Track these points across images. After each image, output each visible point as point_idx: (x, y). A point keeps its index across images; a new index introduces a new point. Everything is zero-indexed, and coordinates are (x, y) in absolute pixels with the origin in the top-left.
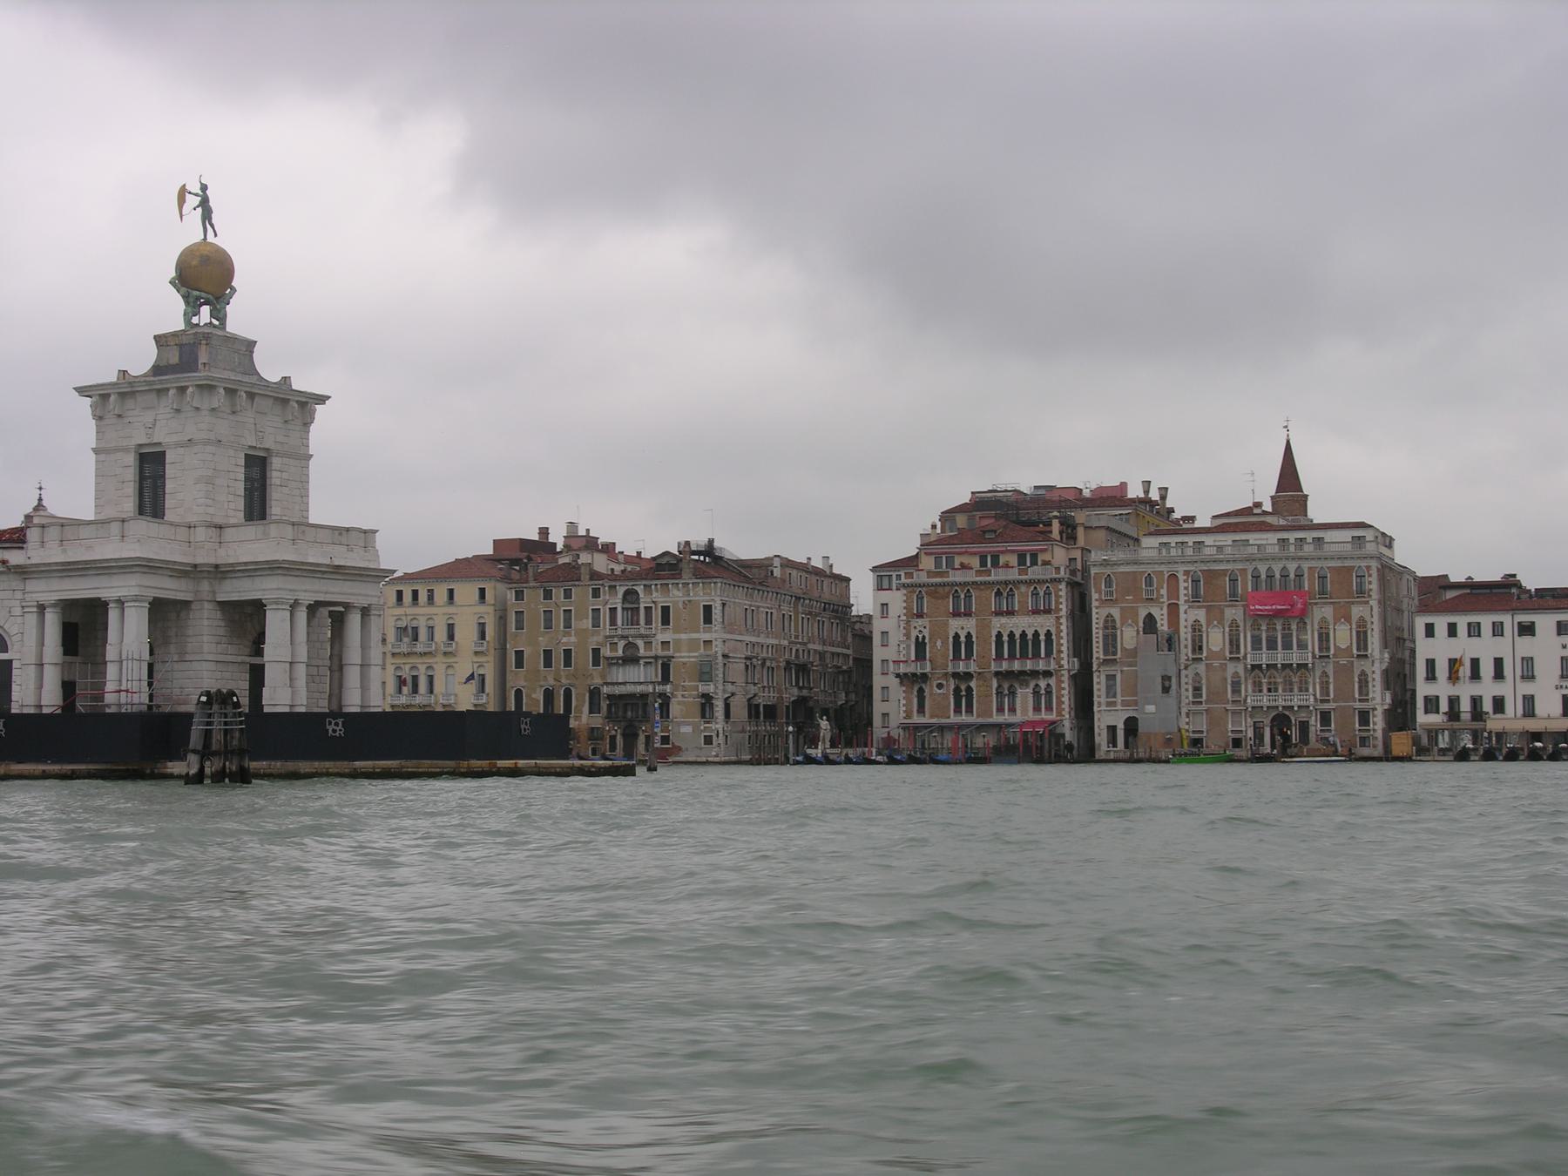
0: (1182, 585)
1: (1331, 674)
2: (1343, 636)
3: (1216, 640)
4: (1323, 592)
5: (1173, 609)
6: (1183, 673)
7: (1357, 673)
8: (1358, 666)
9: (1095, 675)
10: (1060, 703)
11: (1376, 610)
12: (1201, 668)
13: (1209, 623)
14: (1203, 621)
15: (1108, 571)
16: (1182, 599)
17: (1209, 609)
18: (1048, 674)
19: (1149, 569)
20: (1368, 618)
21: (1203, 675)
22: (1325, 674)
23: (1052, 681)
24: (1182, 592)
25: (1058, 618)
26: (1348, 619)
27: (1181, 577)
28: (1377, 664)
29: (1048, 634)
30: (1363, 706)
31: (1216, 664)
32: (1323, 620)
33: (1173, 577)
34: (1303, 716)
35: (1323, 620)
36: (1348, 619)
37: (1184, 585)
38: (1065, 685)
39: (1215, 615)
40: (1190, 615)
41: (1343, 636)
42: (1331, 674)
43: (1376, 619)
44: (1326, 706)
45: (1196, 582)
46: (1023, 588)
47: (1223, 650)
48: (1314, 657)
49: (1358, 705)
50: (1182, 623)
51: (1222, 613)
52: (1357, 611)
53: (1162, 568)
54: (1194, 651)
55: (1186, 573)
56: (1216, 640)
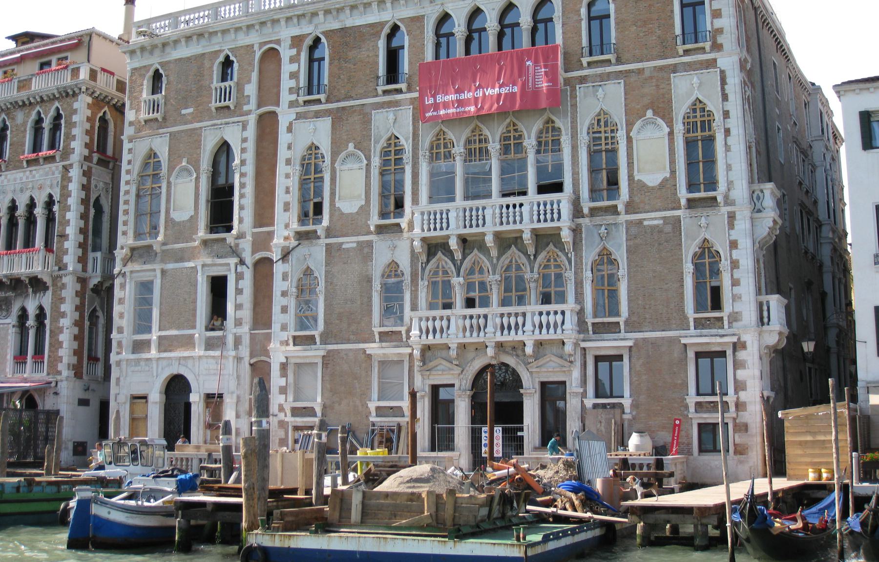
0: (287, 68)
1: (621, 255)
2: (652, 154)
3: (352, 187)
4: (599, 44)
5: (267, 126)
6: (279, 269)
7: (690, 249)
8: (697, 229)
9: (117, 282)
10: (57, 345)
11: (734, 80)
12: (315, 255)
13: (337, 148)
14: (325, 148)
15: (154, 61)
16: (286, 97)
17: (338, 118)
18: (37, 284)
19: (225, 46)
20: (714, 105)
21: (320, 273)
22: (606, 258)
23: (46, 301)
24: (286, 83)
25: (66, 169)
26: (664, 111)
27: (286, 53)
28: (742, 224)
29: (50, 203)
30: (710, 340)
31: (349, 242)
32: (602, 121)
33: (271, 55)
34: (551, 372)
35: (602, 121)
36: (664, 111)
37: (292, 68)
38: (68, 307)
39: (350, 128)
40: (303, 133)
41: (652, 154)
42: (621, 255)
43: (735, 105)
44: (607, 344)
45: (313, 60)
46: (20, 116)
47: (365, 210)
48: (577, 212)
49: (694, 339)
50: (283, 153)
51: (367, 121)
52: (685, 89)
53: (253, 38)
54: (304, 217)
55: (297, 41)
56: (352, 187)
